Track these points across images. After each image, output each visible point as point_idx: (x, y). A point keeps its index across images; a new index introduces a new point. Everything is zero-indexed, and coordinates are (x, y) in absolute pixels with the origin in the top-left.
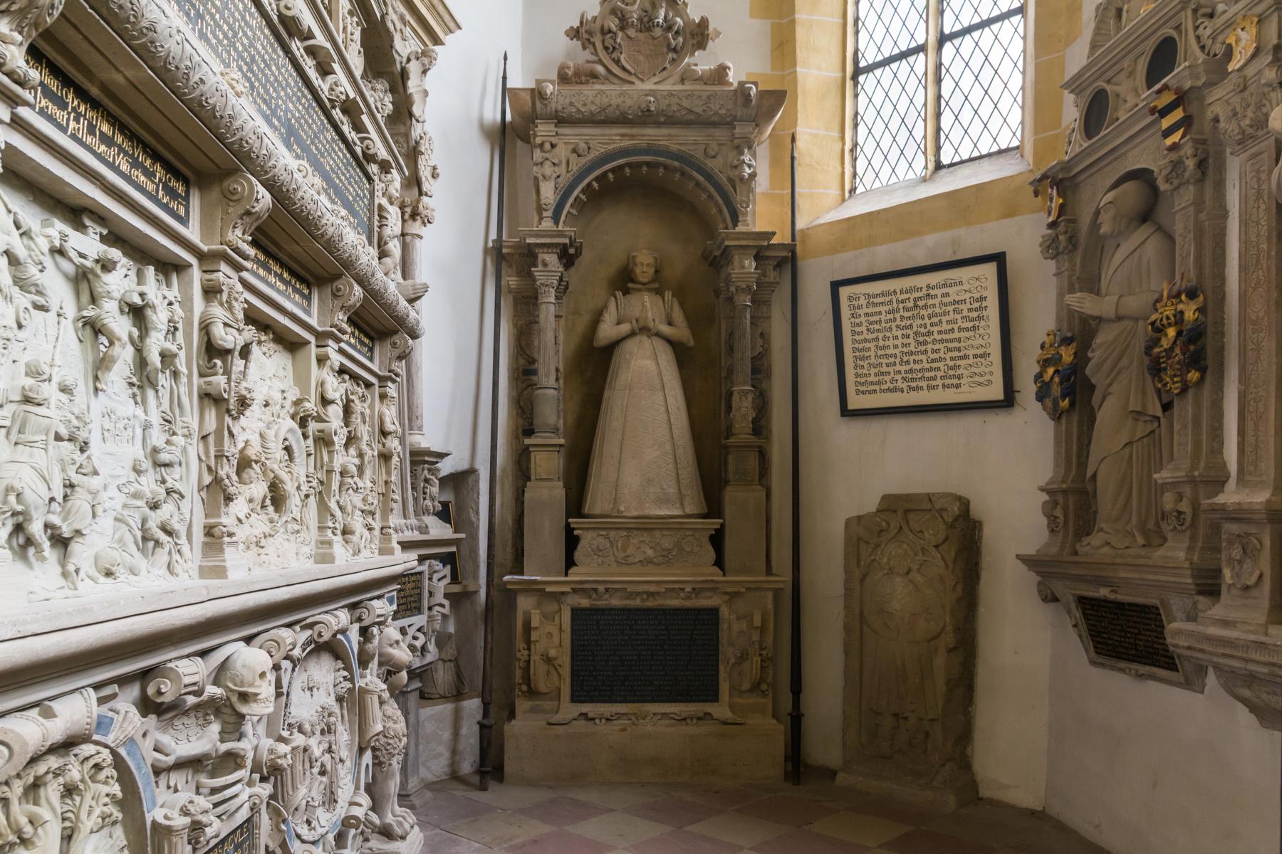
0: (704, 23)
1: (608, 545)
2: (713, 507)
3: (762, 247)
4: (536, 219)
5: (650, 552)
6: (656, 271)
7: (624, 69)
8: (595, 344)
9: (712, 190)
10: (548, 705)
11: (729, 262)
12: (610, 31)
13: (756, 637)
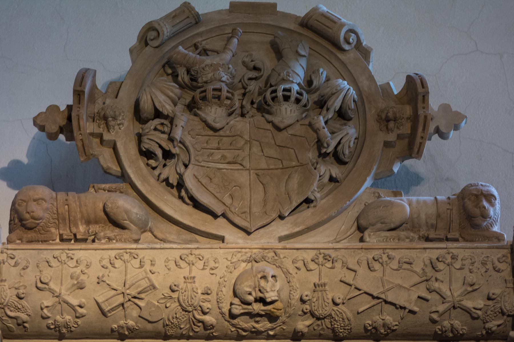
0: (415, 90)
7: (197, 205)
12: (158, 114)
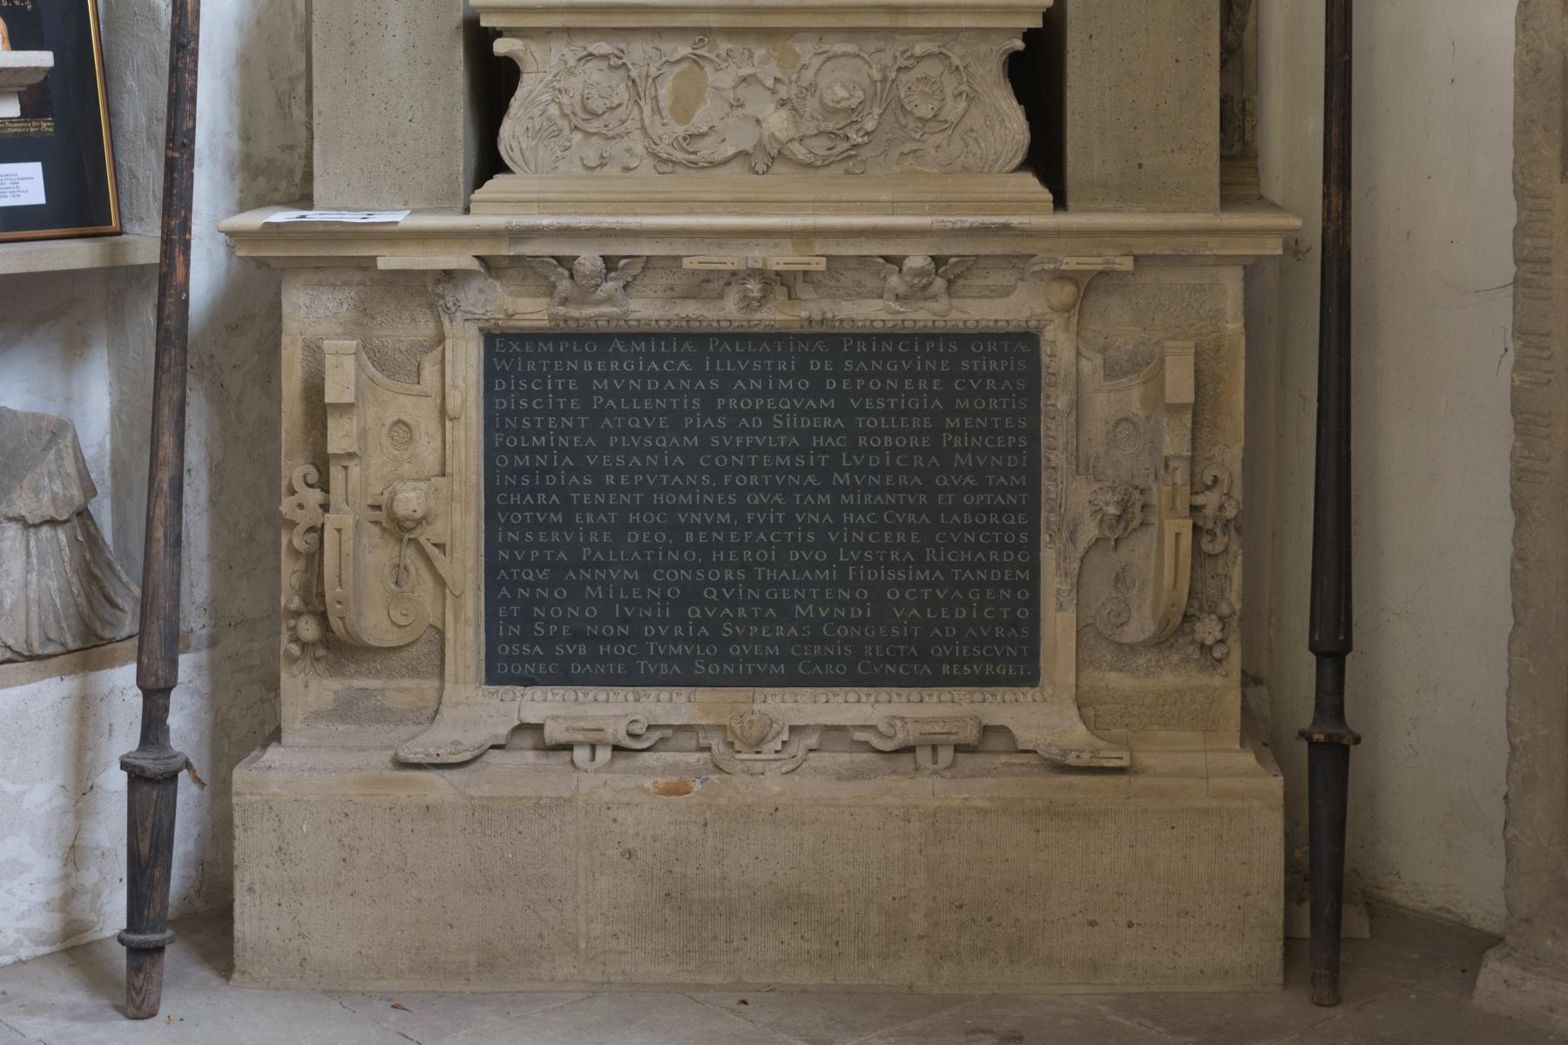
1: (622, 93)
5: (777, 122)
10: (400, 691)
13: (1175, 442)
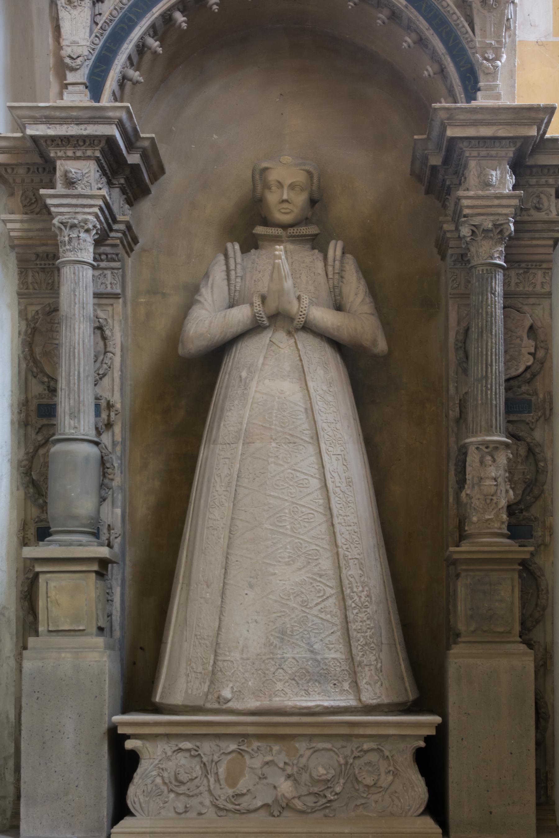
1: (198, 771)
2: (426, 689)
3: (526, 139)
4: (55, 88)
5: (286, 787)
6: (313, 202)
8: (180, 351)
9: (423, 24)
11: (460, 173)
